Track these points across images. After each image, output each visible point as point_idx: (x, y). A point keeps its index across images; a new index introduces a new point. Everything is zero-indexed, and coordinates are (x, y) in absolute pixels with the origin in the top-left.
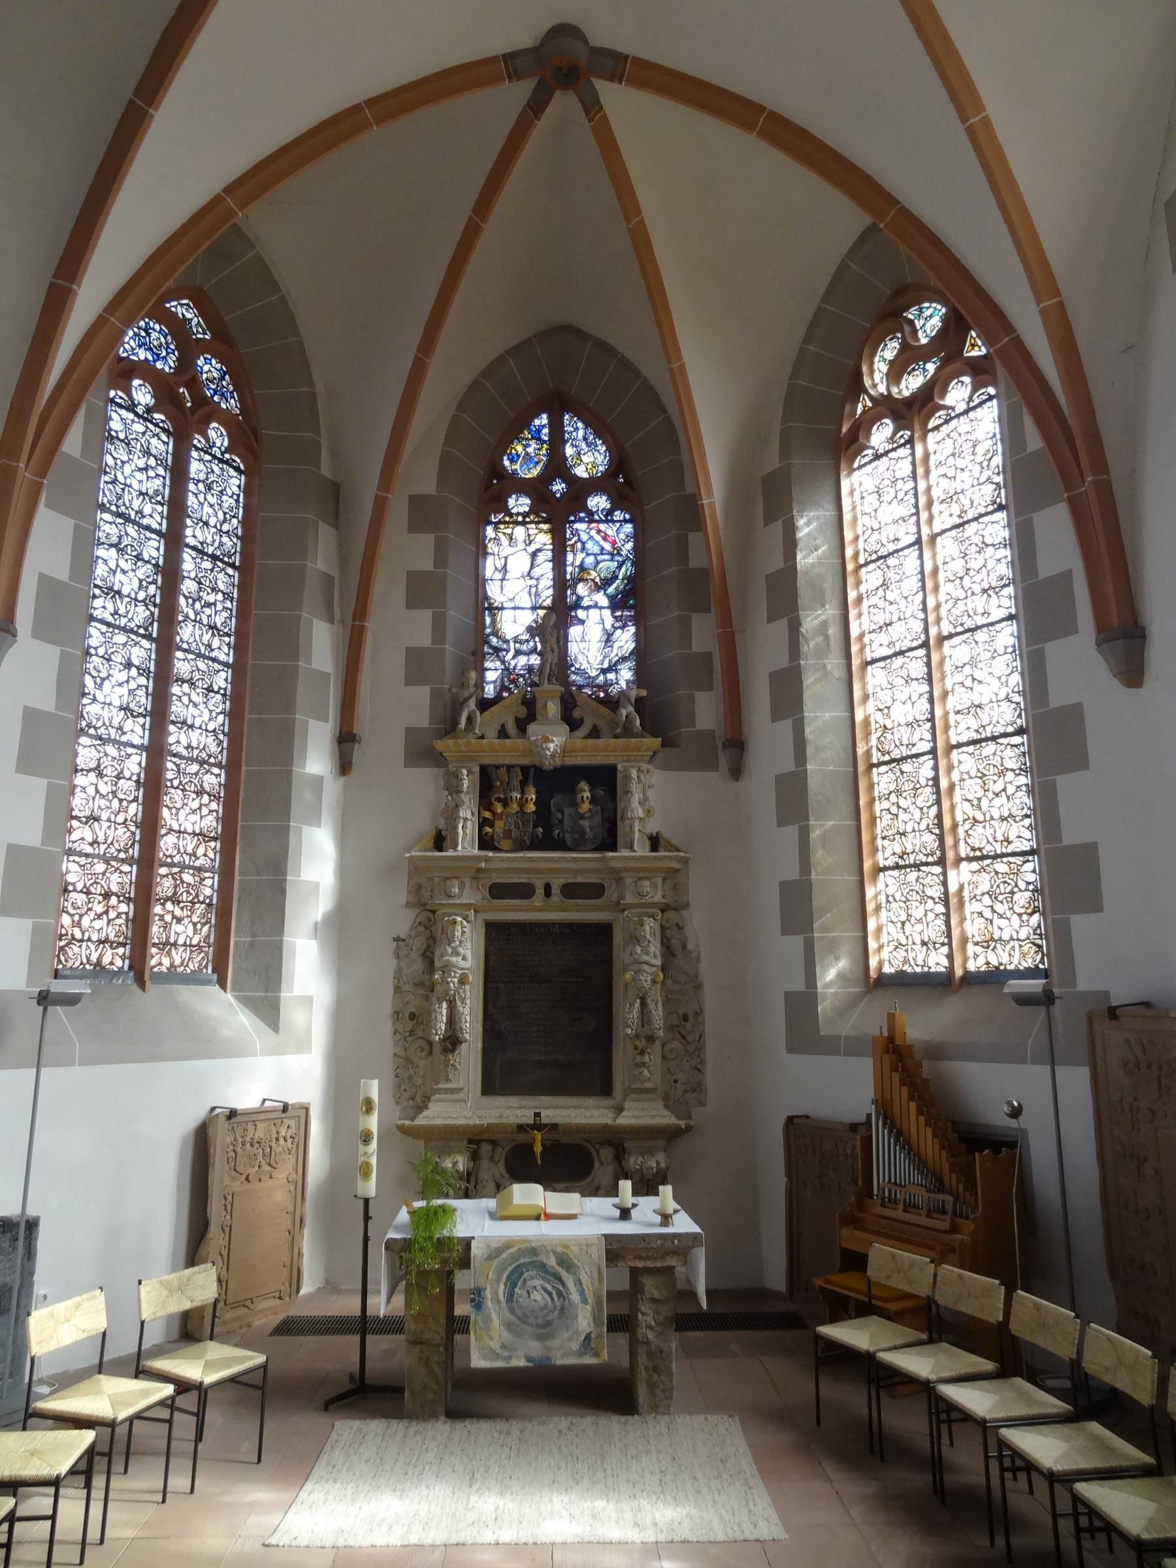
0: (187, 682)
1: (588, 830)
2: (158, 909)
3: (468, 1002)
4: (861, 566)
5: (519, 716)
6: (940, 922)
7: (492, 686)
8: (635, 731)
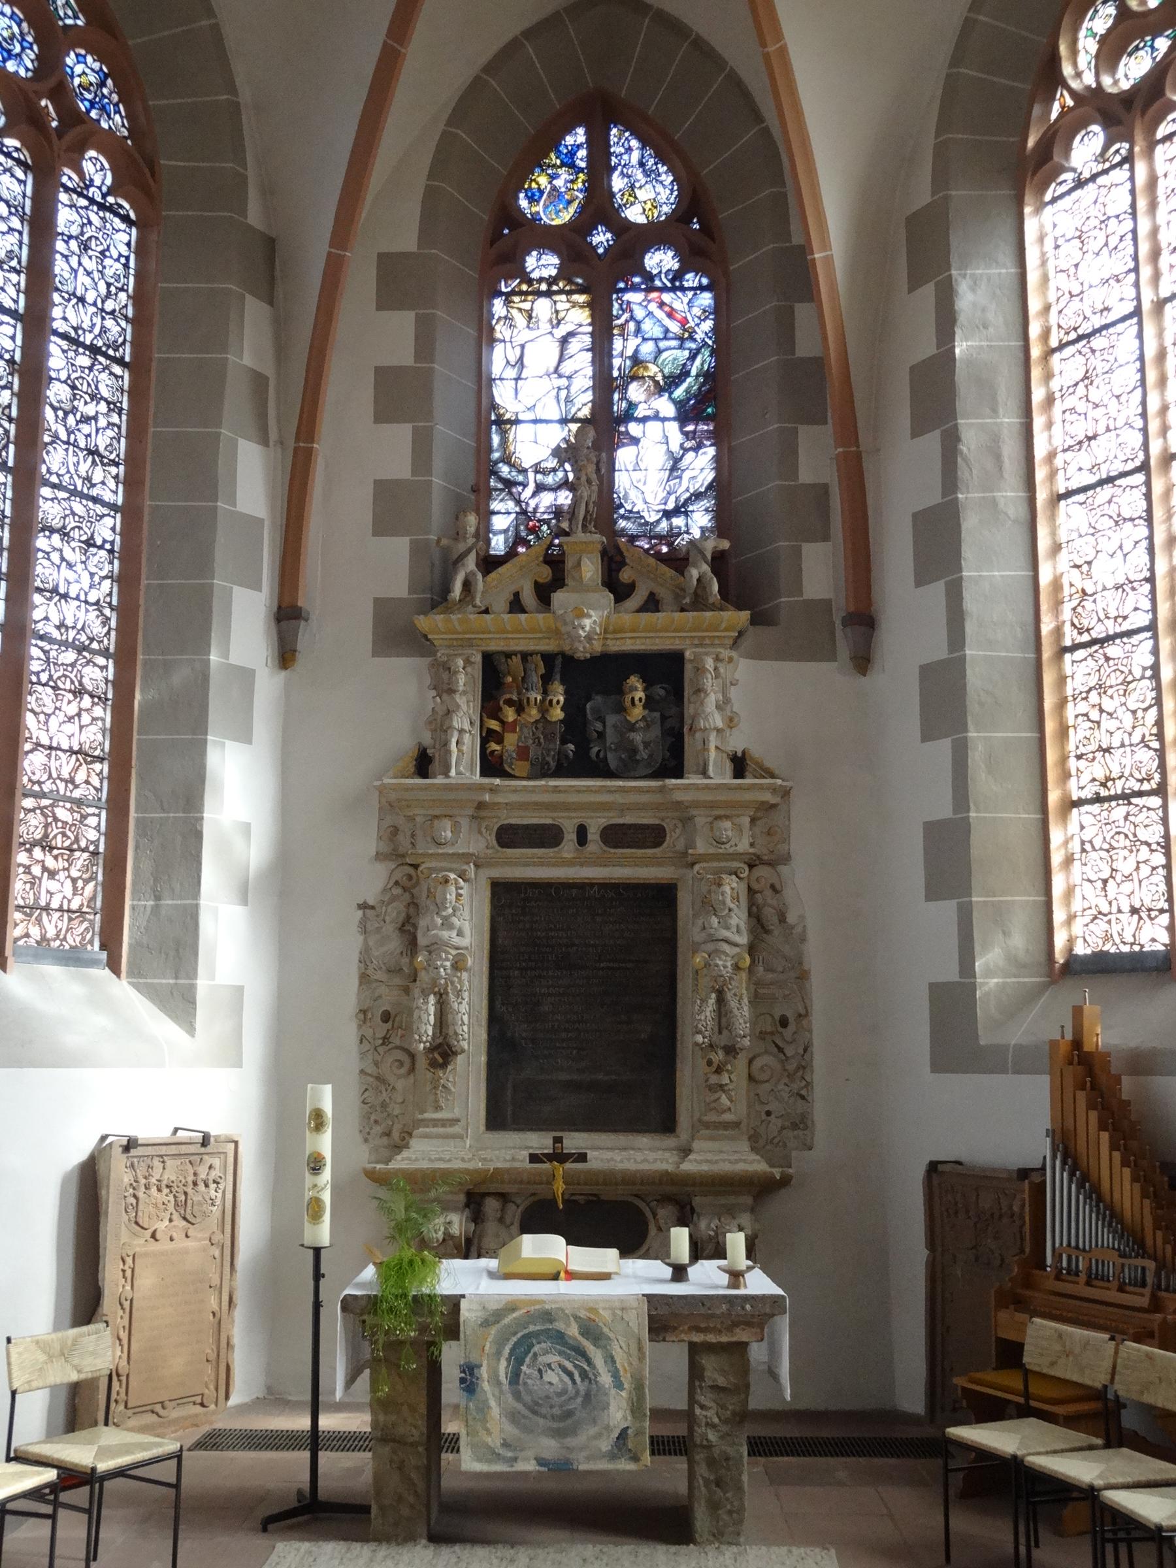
0: (58, 531)
1: (641, 747)
2: (22, 857)
3: (466, 995)
4: (1054, 351)
5: (540, 580)
6: (1159, 877)
7: (501, 538)
8: (711, 600)
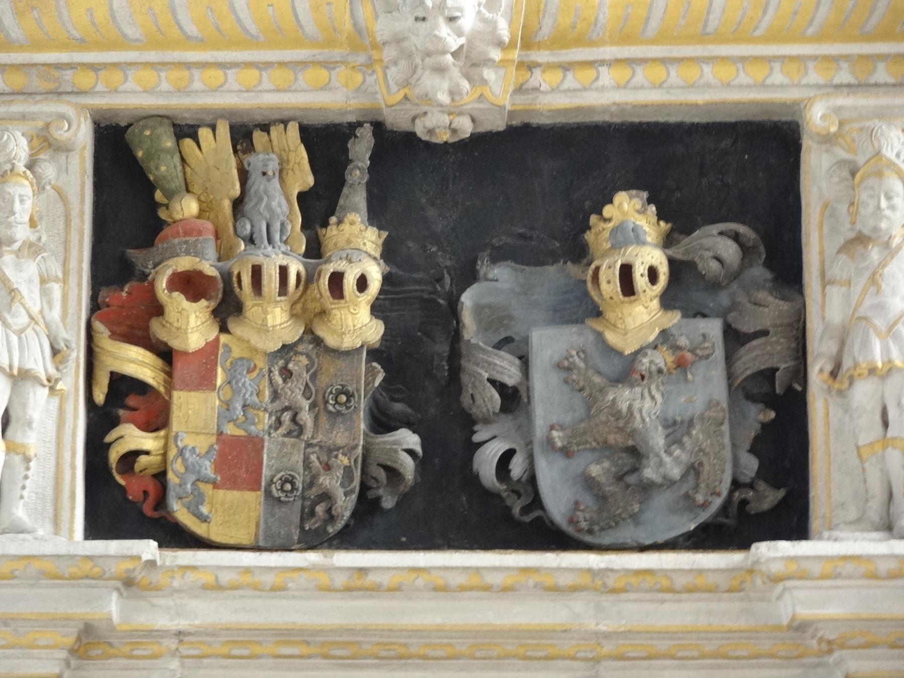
1: (658, 439)
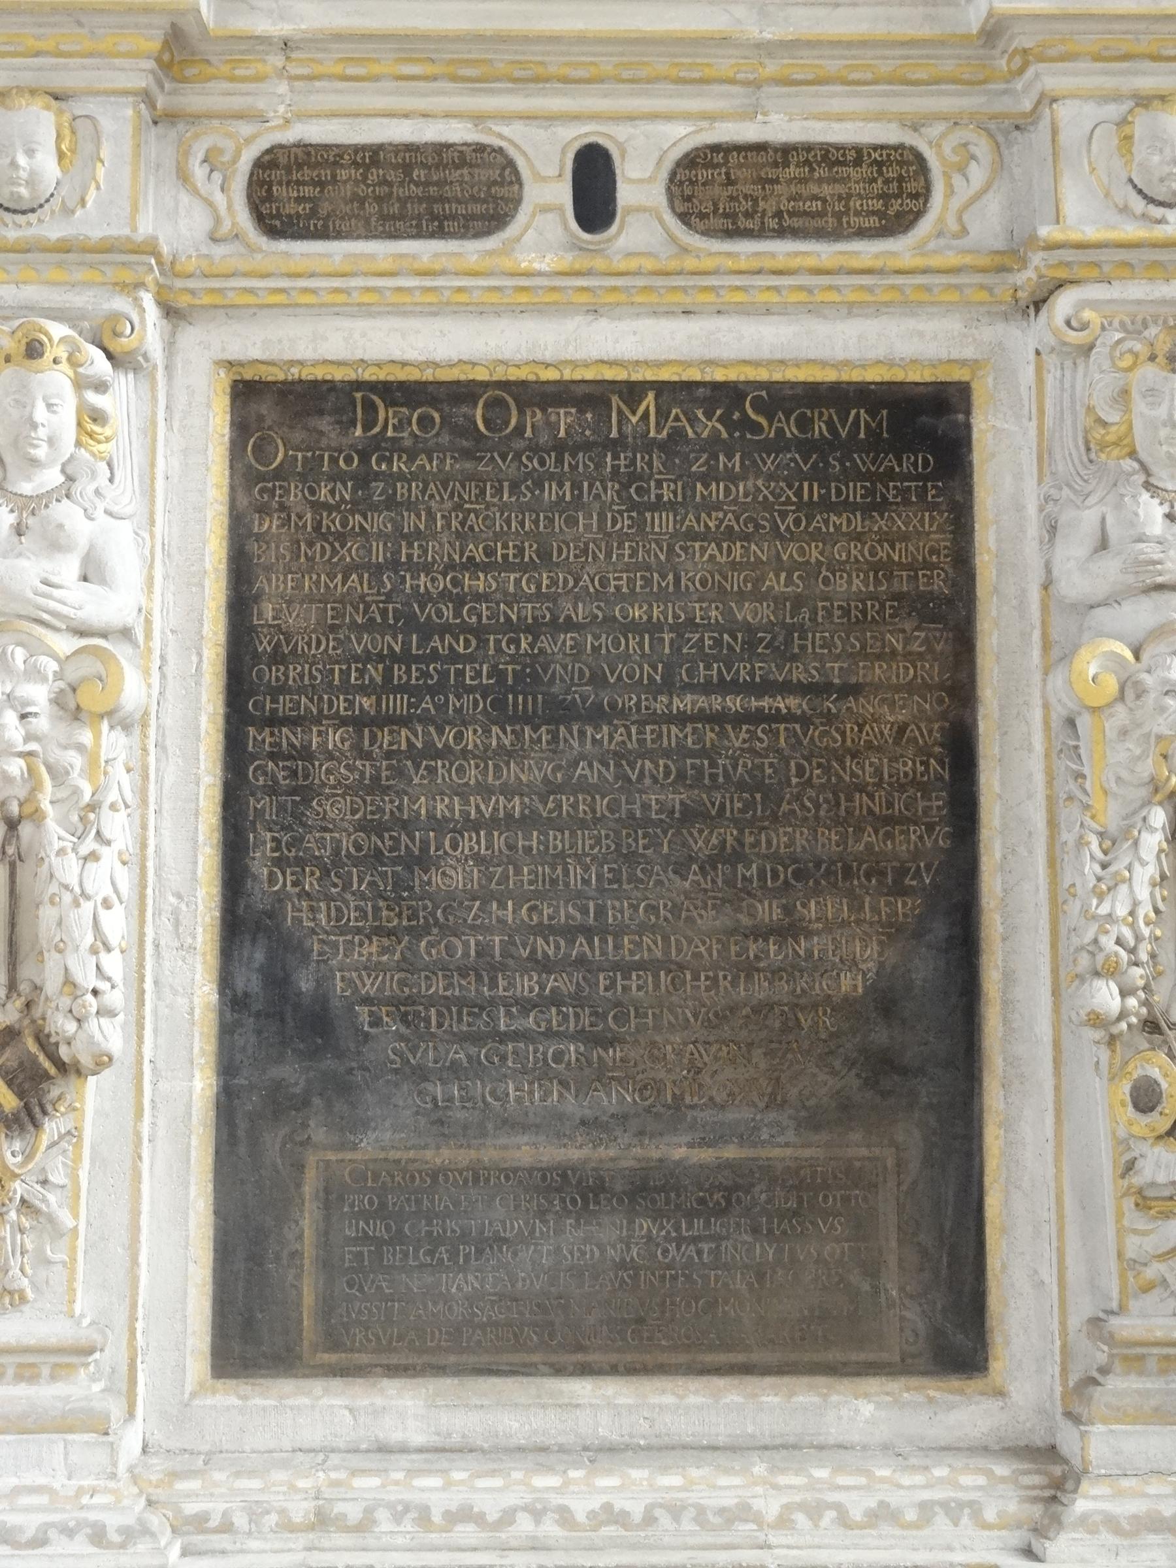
3: (117, 825)
